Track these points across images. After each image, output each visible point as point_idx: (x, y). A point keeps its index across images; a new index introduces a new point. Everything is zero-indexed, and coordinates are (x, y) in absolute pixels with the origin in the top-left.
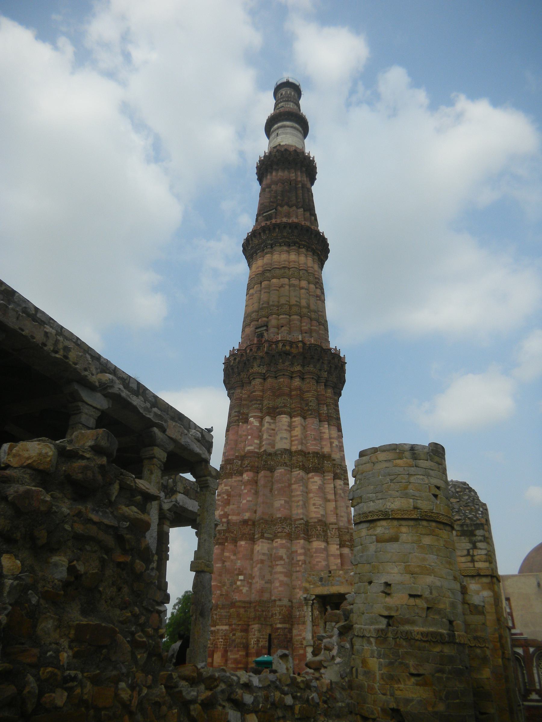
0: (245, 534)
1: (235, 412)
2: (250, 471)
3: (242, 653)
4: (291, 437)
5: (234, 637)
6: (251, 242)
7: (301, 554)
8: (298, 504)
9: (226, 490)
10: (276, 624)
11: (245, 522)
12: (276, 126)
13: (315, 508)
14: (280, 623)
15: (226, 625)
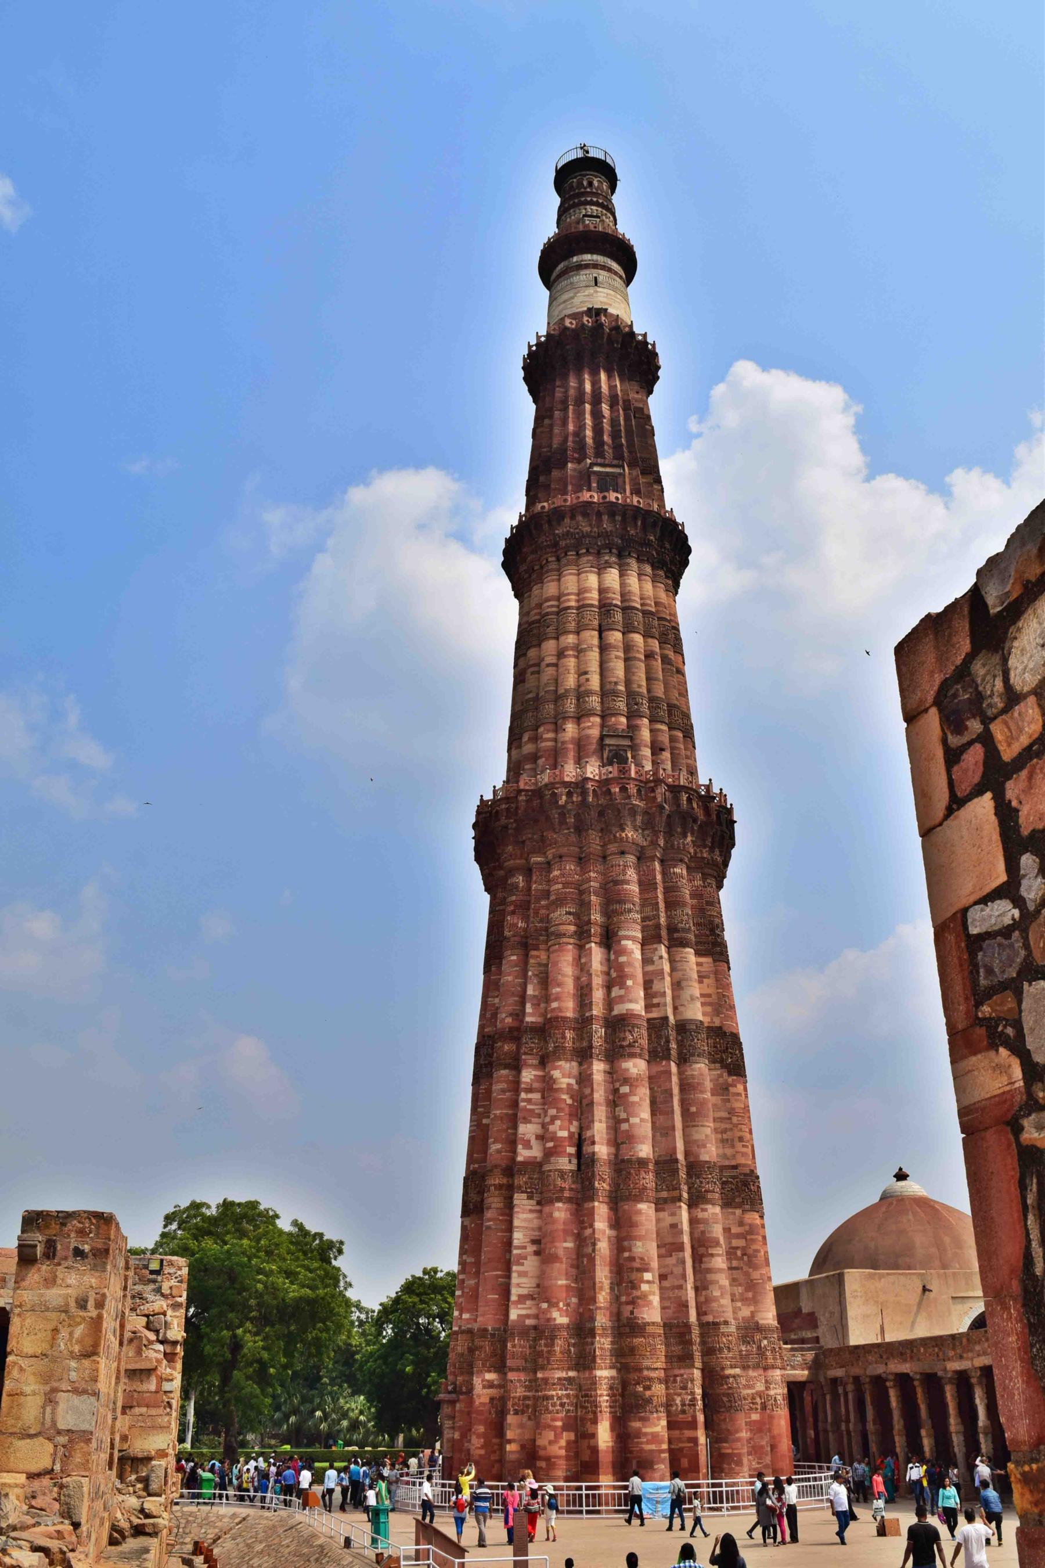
0: (645, 1188)
1: (569, 913)
2: (641, 1056)
3: (664, 1423)
4: (702, 995)
5: (648, 1393)
6: (567, 521)
7: (738, 1236)
8: (725, 1136)
9: (568, 1084)
10: (723, 1369)
11: (642, 1163)
12: (587, 257)
13: (743, 1146)
14: (731, 1367)
15: (611, 1368)
